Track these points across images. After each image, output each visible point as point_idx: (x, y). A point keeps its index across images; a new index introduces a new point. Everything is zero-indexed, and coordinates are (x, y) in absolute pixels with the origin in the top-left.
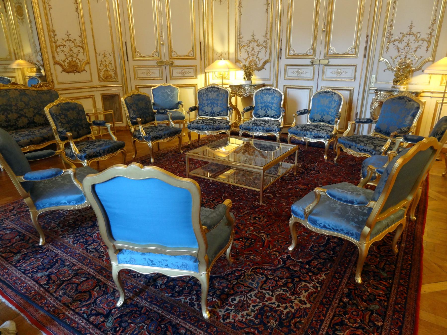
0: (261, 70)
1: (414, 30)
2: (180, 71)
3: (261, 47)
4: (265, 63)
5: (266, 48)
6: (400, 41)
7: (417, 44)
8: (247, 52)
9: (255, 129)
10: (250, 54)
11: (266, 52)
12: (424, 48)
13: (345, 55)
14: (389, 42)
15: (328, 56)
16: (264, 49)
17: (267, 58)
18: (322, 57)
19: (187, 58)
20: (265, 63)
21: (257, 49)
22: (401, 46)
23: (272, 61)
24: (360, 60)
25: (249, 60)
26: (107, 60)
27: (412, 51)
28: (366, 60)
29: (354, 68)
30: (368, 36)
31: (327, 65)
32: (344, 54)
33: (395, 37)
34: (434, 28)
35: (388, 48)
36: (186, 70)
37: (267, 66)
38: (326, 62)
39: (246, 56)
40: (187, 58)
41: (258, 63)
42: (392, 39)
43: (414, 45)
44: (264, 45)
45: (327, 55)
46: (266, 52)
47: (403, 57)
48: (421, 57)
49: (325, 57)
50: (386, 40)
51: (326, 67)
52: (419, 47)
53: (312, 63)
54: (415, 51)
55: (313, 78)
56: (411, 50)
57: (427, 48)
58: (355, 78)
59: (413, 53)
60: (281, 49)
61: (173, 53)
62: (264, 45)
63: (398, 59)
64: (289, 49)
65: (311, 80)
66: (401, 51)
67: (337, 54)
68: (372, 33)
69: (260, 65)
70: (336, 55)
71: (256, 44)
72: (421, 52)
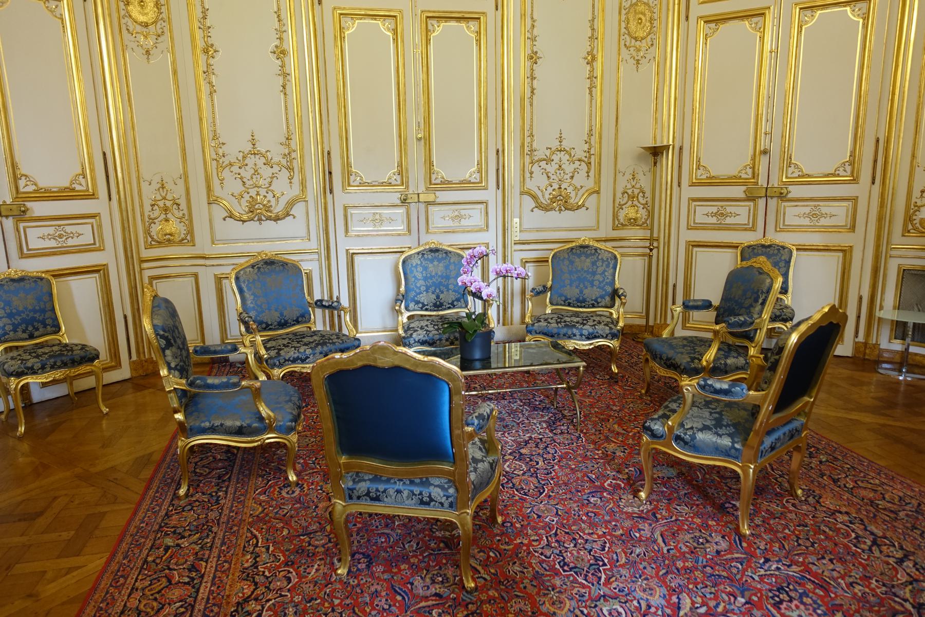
0: (284, 218)
1: (566, 144)
2: (51, 230)
3: (276, 169)
4: (291, 204)
5: (290, 169)
6: (549, 161)
7: (573, 167)
8: (241, 178)
9: (564, 335)
10: (248, 183)
11: (291, 179)
12: (583, 173)
13: (465, 185)
14: (532, 163)
15: (432, 185)
16: (285, 174)
17: (296, 191)
18: (422, 189)
19: (67, 194)
20: (291, 204)
21: (266, 172)
22: (552, 168)
23: (310, 198)
24: (490, 194)
25: (247, 197)
26: (169, 197)
27: (568, 177)
28: (500, 192)
29: (482, 206)
30: (498, 151)
31: (433, 203)
32: (461, 182)
33: (539, 155)
34: (593, 143)
35: (531, 173)
36: (69, 229)
37: (298, 210)
38: (431, 198)
39: (238, 188)
40: (67, 194)
41: (273, 203)
42: (536, 158)
43: (569, 168)
44: (284, 162)
45: (431, 184)
46: (291, 179)
47: (556, 186)
48: (582, 187)
49: (427, 189)
50: (527, 160)
51: (430, 207)
52: (575, 171)
53: (404, 201)
54: (572, 177)
55: (409, 231)
56: (566, 177)
57: (588, 172)
58: (487, 227)
59: (569, 180)
60: (330, 173)
61: (22, 183)
62: (284, 162)
63: (550, 190)
64: (350, 174)
65: (404, 235)
66: (552, 177)
67: (449, 182)
68: (503, 145)
69: (278, 209)
70: (447, 185)
71: (263, 160)
72: (580, 179)
